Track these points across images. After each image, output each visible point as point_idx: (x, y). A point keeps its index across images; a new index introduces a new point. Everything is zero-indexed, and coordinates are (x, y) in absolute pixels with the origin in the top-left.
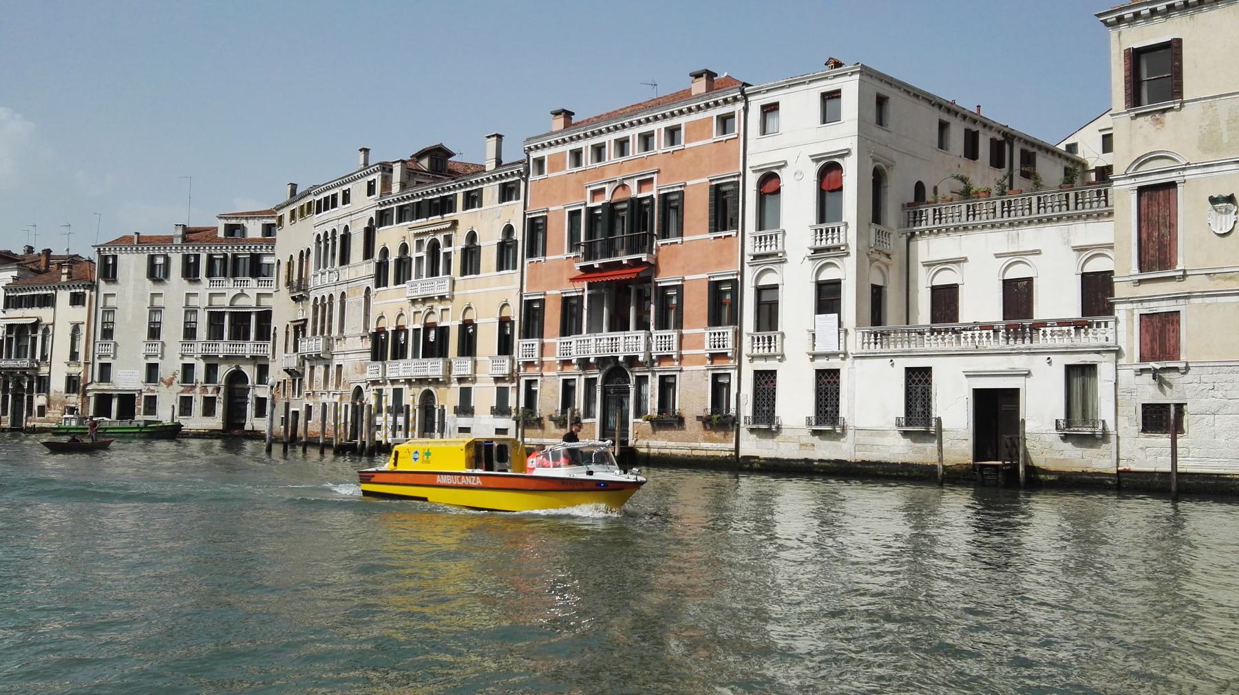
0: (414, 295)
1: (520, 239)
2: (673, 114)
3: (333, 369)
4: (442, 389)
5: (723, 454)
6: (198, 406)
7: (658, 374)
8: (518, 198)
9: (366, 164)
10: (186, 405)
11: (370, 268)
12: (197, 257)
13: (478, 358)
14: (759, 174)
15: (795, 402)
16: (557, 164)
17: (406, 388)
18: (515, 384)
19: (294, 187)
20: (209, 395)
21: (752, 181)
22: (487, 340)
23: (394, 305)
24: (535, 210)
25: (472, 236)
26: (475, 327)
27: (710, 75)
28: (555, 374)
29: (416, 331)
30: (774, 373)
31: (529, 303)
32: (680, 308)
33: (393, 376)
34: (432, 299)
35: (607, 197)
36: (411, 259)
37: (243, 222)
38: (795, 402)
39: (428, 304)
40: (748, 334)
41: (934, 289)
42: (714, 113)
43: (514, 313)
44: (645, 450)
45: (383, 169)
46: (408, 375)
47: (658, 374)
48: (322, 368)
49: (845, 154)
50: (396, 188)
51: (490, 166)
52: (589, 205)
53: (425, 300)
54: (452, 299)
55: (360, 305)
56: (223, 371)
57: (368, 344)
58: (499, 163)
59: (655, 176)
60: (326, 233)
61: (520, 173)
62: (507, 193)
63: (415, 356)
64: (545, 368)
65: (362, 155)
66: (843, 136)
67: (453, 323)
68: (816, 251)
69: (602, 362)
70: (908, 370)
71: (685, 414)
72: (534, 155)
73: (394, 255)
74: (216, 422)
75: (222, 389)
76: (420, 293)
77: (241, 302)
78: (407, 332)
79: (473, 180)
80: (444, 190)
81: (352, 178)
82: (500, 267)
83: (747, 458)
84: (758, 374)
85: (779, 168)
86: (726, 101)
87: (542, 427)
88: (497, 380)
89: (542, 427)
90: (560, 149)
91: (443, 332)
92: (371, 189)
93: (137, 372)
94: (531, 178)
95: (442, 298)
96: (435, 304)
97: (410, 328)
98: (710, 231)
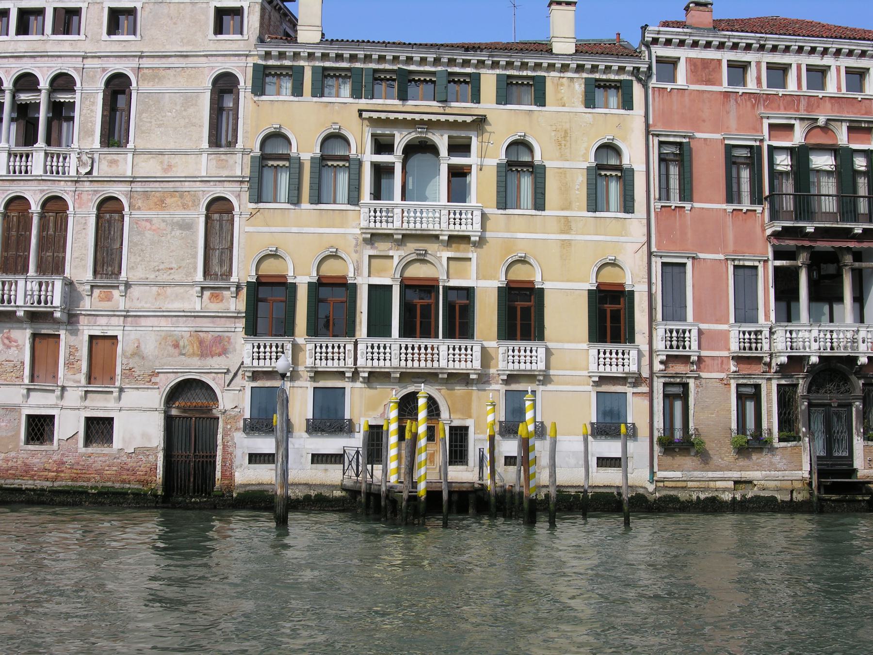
0: (383, 227)
1: (639, 168)
3: (72, 345)
4: (460, 390)
11: (239, 166)
18: (644, 389)
24: (676, 133)
29: (379, 294)
36: (360, 163)
53: (407, 237)
57: (238, 304)
67: (484, 281)
72: (660, 51)
79: (531, 62)
82: (595, 203)
88: (604, 380)
89: (704, 456)
94: (653, 82)
97: (363, 282)
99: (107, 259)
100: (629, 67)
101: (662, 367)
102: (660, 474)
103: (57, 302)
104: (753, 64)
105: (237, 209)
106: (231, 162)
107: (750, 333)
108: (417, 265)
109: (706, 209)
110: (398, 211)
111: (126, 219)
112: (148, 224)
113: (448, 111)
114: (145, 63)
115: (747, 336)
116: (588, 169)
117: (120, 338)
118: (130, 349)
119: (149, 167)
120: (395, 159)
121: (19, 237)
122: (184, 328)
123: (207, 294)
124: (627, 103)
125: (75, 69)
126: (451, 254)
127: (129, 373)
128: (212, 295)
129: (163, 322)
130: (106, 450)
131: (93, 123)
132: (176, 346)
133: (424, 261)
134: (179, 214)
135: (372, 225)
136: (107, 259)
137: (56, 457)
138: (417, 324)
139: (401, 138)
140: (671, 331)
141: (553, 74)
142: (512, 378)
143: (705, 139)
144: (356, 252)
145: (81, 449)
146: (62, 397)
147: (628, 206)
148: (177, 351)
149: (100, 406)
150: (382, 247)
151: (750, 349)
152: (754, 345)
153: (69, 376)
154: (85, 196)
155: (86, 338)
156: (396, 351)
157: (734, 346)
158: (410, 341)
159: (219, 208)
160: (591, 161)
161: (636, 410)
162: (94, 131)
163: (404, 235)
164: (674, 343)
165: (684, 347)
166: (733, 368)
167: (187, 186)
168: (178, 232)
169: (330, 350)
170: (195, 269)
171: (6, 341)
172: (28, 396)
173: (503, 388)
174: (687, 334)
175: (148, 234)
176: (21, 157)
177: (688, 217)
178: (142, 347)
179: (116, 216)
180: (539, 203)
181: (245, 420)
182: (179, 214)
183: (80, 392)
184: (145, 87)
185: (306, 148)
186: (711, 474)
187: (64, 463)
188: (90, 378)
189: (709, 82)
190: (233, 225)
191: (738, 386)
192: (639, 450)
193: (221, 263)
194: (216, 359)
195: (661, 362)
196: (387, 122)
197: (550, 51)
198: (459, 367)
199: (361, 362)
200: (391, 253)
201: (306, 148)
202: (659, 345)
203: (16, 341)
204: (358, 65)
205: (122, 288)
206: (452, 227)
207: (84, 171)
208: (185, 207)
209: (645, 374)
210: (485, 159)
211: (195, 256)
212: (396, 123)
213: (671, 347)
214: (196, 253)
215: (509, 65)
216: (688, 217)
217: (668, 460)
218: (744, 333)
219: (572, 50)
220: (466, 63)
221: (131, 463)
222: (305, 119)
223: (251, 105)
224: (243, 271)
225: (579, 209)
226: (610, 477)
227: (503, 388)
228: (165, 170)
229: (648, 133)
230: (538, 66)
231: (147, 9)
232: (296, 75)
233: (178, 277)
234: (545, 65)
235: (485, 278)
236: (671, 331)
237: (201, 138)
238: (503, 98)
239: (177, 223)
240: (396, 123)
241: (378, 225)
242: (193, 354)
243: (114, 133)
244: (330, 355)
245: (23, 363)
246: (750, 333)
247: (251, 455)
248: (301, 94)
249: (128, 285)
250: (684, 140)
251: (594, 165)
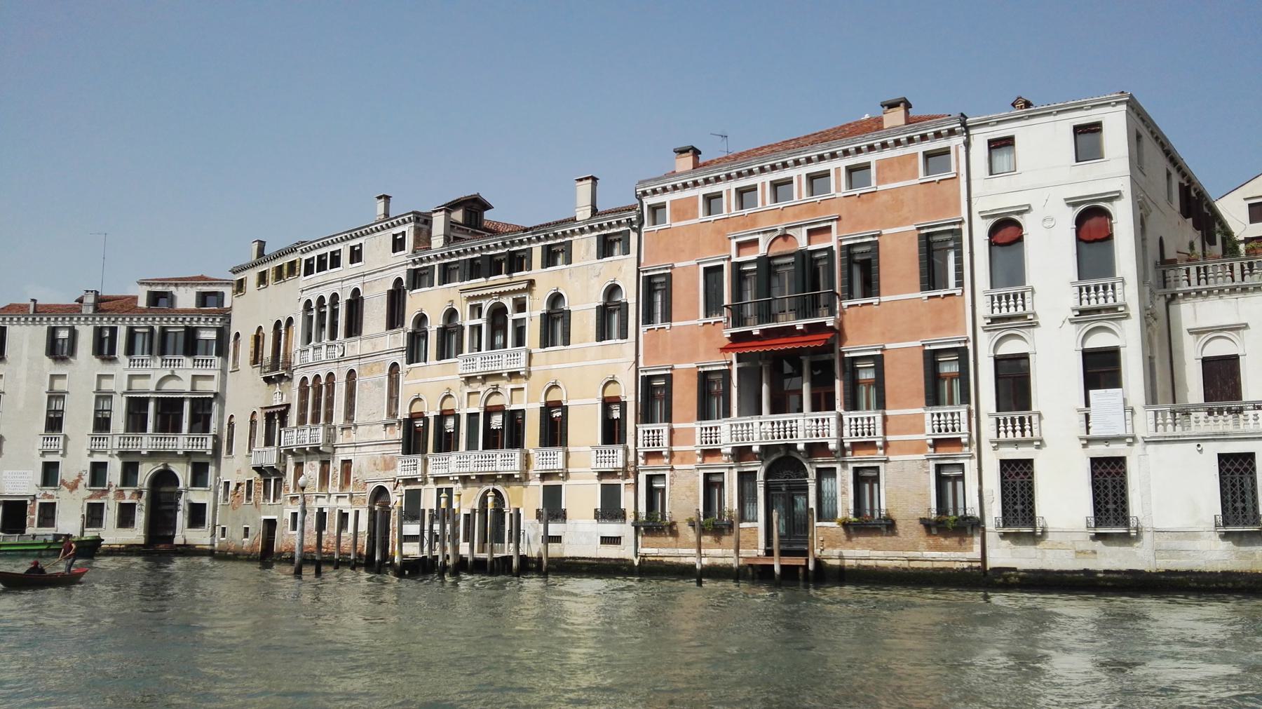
0: (471, 372)
1: (632, 301)
2: (858, 150)
3: (335, 466)
4: (515, 488)
5: (957, 565)
6: (111, 515)
7: (851, 466)
8: (626, 251)
9: (386, 215)
10: (94, 515)
11: (400, 339)
12: (114, 331)
13: (570, 449)
14: (991, 222)
15: (1063, 499)
16: (682, 211)
17: (457, 488)
19: (262, 245)
20: (127, 501)
21: (981, 229)
22: (585, 426)
23: (435, 385)
24: (654, 265)
25: (556, 298)
26: (565, 410)
27: (697, 153)
28: (693, 466)
29: (472, 417)
30: (1029, 463)
31: (647, 380)
32: (879, 383)
33: (441, 472)
34: (498, 376)
35: (762, 250)
36: (462, 328)
37: (172, 289)
38: (1063, 499)
39: (489, 384)
40: (990, 415)
41: (1205, 361)
42: (920, 149)
43: (627, 391)
44: (837, 562)
45: (417, 220)
46: (465, 471)
47: (851, 466)
48: (317, 465)
49: (1114, 197)
50: (437, 242)
51: (583, 213)
52: (735, 259)
53: (485, 378)
54: (528, 376)
55: (380, 384)
56: (146, 471)
57: (398, 434)
58: (594, 211)
59: (834, 224)
60: (321, 299)
61: (630, 222)
62: (606, 247)
63: (471, 445)
64: (676, 459)
65: (381, 205)
66: (1111, 174)
67: (530, 405)
68: (1082, 312)
69: (766, 450)
70: (1221, 456)
71: (896, 515)
72: (648, 201)
73: (435, 323)
74: (136, 534)
75: (145, 494)
76: (479, 369)
77: (170, 385)
78: (457, 418)
79: (559, 232)
80: (513, 243)
81: (367, 231)
82: (603, 333)
83: (999, 571)
84: (1005, 464)
85: (1020, 213)
86: (938, 135)
87: (674, 533)
88: (602, 475)
89: (674, 533)
90: (688, 193)
91: (515, 421)
92: (398, 244)
93: (30, 473)
94: (646, 228)
95: (513, 375)
96: (502, 383)
97: (464, 412)
98: (923, 289)
100: (624, 221)
102: (642, 551)
108: (495, 396)
120: (483, 321)
133: (498, 393)
138: (492, 440)
139: (486, 305)
141: (576, 237)
142: (544, 476)
150: (475, 386)
161: (627, 501)
173: (541, 484)
180: (567, 342)
186: (681, 551)
192: (624, 529)
196: (478, 297)
198: (508, 469)
212: (483, 297)
215: (547, 237)
217: (648, 539)
220: (521, 242)
224: (403, 413)
226: (611, 552)
227: (541, 484)
229: (638, 271)
230: (564, 234)
233: (377, 419)
240: (483, 297)
249: (356, 426)
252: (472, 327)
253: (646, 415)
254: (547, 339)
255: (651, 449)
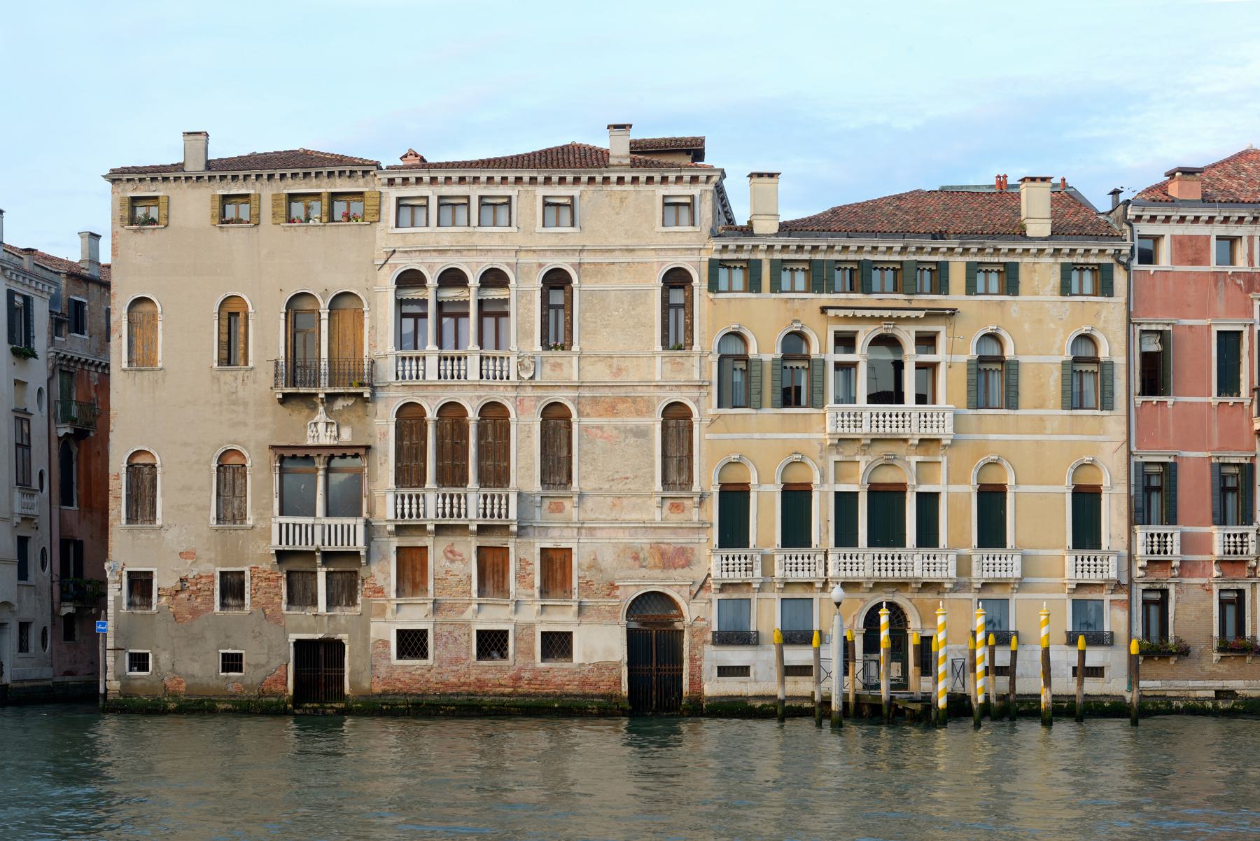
0: (851, 432)
1: (1120, 360)
3: (524, 556)
46: (852, 575)
88: (1080, 586)
90: (1200, 230)
96: (899, 449)
99: (556, 466)
100: (1110, 251)
101: (1141, 573)
103: (513, 515)
104: (1245, 239)
105: (696, 416)
106: (687, 365)
107: (1235, 536)
109: (1191, 404)
110: (866, 415)
111: (575, 427)
112: (599, 433)
113: (914, 305)
114: (586, 258)
115: (1232, 539)
116: (1063, 363)
117: (574, 551)
118: (586, 561)
119: (597, 372)
121: (454, 444)
122: (643, 541)
123: (668, 503)
124: (1105, 288)
125: (508, 264)
126: (919, 458)
127: (586, 586)
128: (672, 505)
129: (620, 534)
130: (566, 665)
131: (532, 324)
132: (636, 558)
134: (633, 421)
135: (840, 430)
136: (556, 466)
137: (511, 673)
138: (886, 532)
139: (864, 335)
140: (1152, 535)
141: (1026, 259)
142: (986, 585)
143: (1191, 327)
144: (821, 458)
145: (539, 663)
146: (516, 611)
147: (1106, 403)
148: (637, 563)
149: (559, 621)
150: (849, 451)
151: (1235, 552)
152: (1239, 549)
153: (521, 590)
154: (527, 403)
155: (538, 551)
156: (867, 561)
157: (1218, 551)
158: (877, 551)
159: (677, 416)
160: (1068, 356)
161: (1114, 620)
162: (532, 332)
163: (873, 440)
164: (1156, 548)
165: (1166, 552)
166: (1216, 573)
167: (640, 392)
168: (632, 440)
169: (800, 560)
170: (653, 478)
171: (450, 555)
172: (479, 610)
174: (1169, 539)
175: (600, 442)
176: (452, 359)
177: (1171, 413)
178: (599, 559)
179: (562, 423)
181: (714, 633)
182: (633, 421)
183: (537, 606)
184: (589, 285)
185: (765, 348)
186: (1191, 684)
187: (521, 678)
188: (544, 592)
189: (1195, 262)
190: (691, 431)
191: (1221, 591)
193: (680, 472)
194: (680, 571)
195: (1141, 568)
197: (1023, 236)
199: (831, 573)
200: (857, 458)
201: (765, 348)
202: (1140, 550)
203: (460, 555)
204: (819, 257)
205: (576, 499)
206: (923, 430)
207: (526, 376)
208: (639, 413)
209: (1125, 581)
210: (954, 355)
211: (652, 465)
213: (1152, 552)
214: (653, 462)
216: (1171, 413)
218: (1229, 536)
219: (1047, 233)
221: (593, 678)
222: (764, 321)
223: (707, 304)
225: (1055, 408)
228: (615, 375)
229: (1129, 321)
231: (586, 198)
232: (752, 268)
234: (1019, 251)
235: (955, 483)
236: (1152, 535)
237: (652, 339)
238: (971, 289)
239: (631, 430)
241: (846, 430)
242: (655, 567)
243: (556, 334)
244: (800, 565)
245: (470, 577)
246: (1235, 536)
247: (719, 668)
248: (759, 290)
249: (581, 496)
250: (1168, 328)
251: (1071, 358)
252: (839, 366)
253: (1138, 515)
254: (979, 398)
255: (1156, 557)
